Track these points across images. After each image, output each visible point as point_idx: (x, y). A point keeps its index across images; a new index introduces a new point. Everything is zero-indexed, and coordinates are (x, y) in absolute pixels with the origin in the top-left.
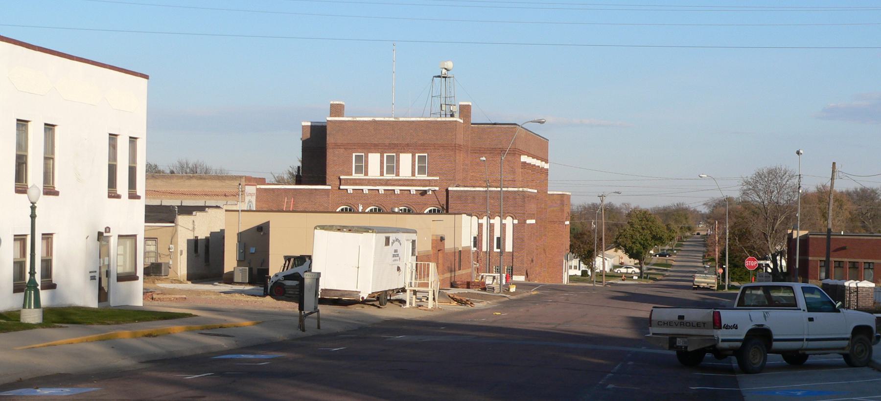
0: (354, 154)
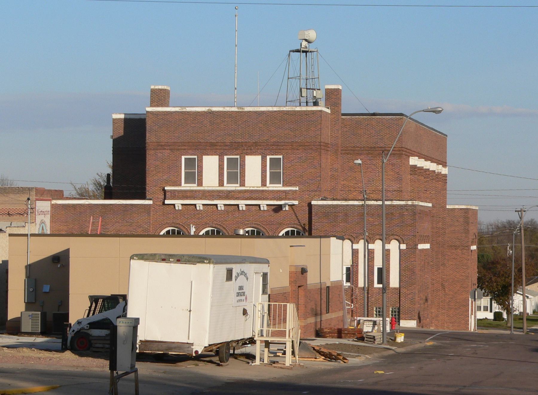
0: (183, 158)
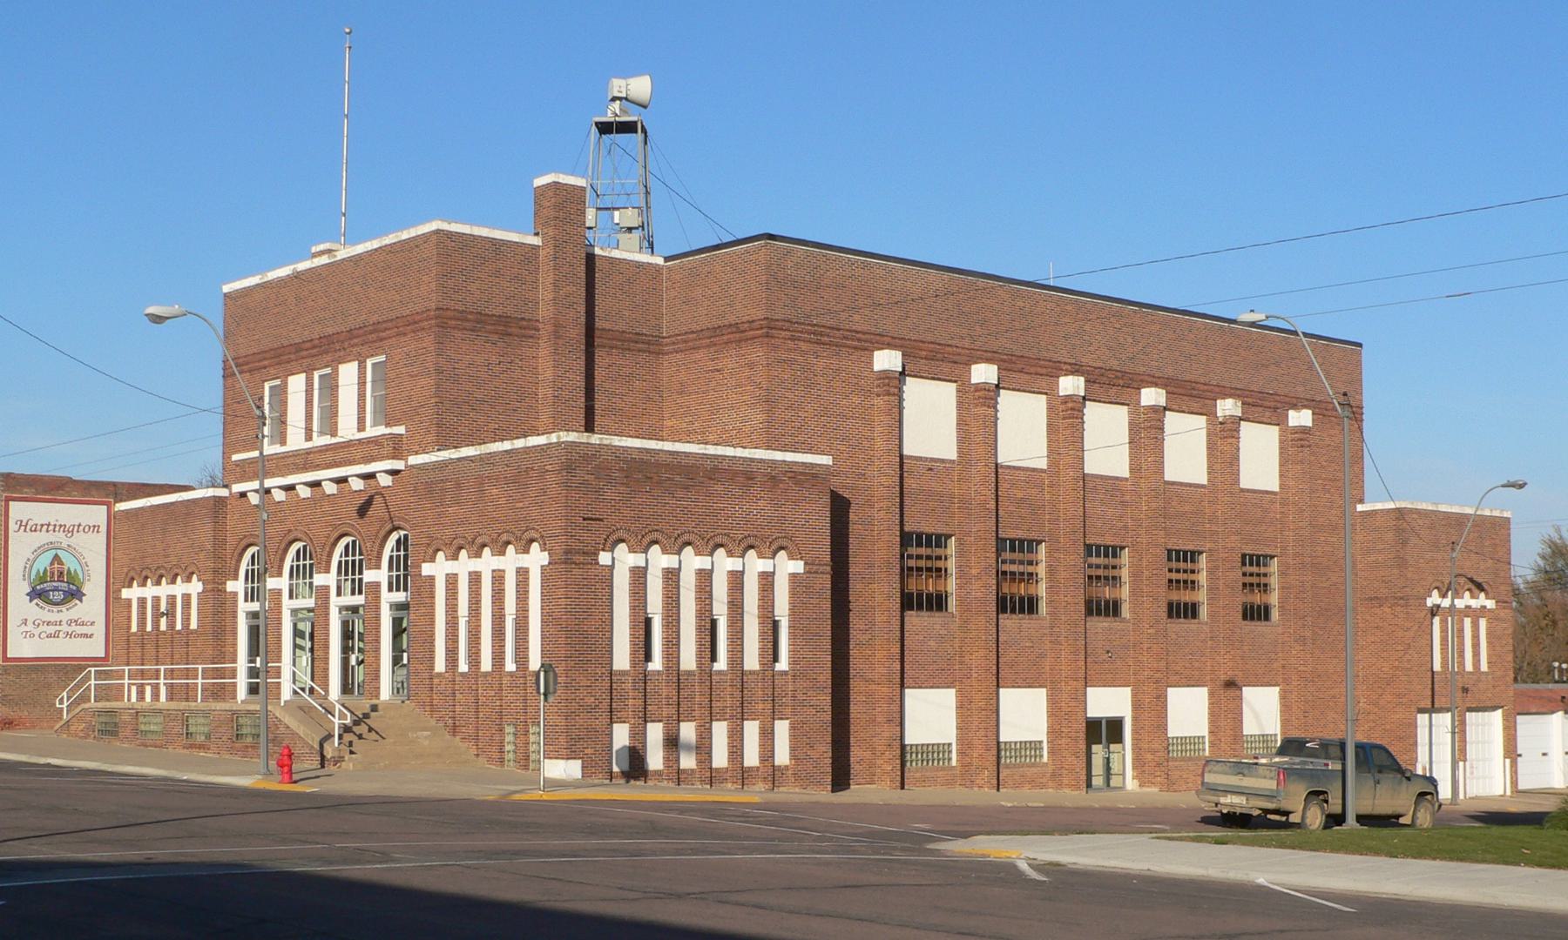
0: (267, 386)
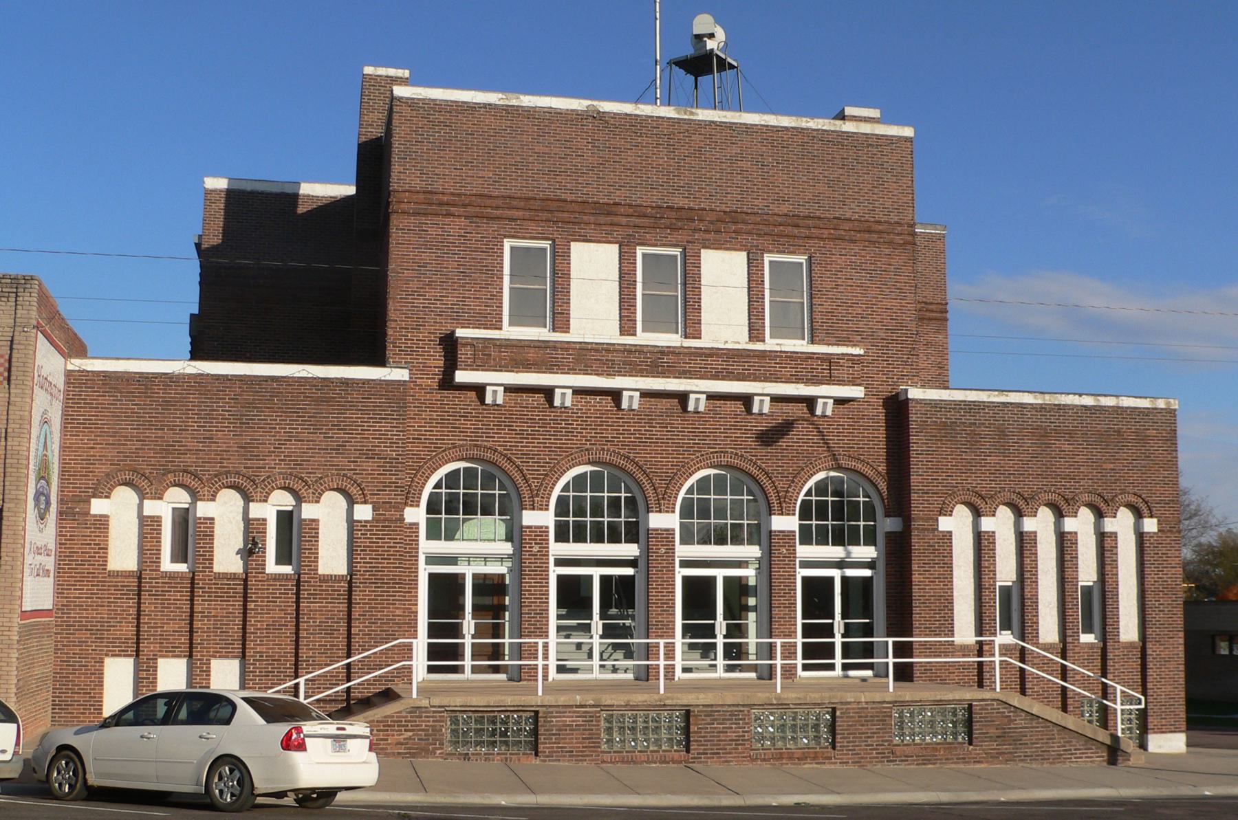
0: (508, 244)
